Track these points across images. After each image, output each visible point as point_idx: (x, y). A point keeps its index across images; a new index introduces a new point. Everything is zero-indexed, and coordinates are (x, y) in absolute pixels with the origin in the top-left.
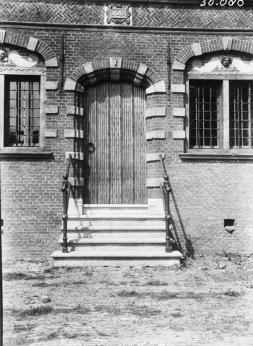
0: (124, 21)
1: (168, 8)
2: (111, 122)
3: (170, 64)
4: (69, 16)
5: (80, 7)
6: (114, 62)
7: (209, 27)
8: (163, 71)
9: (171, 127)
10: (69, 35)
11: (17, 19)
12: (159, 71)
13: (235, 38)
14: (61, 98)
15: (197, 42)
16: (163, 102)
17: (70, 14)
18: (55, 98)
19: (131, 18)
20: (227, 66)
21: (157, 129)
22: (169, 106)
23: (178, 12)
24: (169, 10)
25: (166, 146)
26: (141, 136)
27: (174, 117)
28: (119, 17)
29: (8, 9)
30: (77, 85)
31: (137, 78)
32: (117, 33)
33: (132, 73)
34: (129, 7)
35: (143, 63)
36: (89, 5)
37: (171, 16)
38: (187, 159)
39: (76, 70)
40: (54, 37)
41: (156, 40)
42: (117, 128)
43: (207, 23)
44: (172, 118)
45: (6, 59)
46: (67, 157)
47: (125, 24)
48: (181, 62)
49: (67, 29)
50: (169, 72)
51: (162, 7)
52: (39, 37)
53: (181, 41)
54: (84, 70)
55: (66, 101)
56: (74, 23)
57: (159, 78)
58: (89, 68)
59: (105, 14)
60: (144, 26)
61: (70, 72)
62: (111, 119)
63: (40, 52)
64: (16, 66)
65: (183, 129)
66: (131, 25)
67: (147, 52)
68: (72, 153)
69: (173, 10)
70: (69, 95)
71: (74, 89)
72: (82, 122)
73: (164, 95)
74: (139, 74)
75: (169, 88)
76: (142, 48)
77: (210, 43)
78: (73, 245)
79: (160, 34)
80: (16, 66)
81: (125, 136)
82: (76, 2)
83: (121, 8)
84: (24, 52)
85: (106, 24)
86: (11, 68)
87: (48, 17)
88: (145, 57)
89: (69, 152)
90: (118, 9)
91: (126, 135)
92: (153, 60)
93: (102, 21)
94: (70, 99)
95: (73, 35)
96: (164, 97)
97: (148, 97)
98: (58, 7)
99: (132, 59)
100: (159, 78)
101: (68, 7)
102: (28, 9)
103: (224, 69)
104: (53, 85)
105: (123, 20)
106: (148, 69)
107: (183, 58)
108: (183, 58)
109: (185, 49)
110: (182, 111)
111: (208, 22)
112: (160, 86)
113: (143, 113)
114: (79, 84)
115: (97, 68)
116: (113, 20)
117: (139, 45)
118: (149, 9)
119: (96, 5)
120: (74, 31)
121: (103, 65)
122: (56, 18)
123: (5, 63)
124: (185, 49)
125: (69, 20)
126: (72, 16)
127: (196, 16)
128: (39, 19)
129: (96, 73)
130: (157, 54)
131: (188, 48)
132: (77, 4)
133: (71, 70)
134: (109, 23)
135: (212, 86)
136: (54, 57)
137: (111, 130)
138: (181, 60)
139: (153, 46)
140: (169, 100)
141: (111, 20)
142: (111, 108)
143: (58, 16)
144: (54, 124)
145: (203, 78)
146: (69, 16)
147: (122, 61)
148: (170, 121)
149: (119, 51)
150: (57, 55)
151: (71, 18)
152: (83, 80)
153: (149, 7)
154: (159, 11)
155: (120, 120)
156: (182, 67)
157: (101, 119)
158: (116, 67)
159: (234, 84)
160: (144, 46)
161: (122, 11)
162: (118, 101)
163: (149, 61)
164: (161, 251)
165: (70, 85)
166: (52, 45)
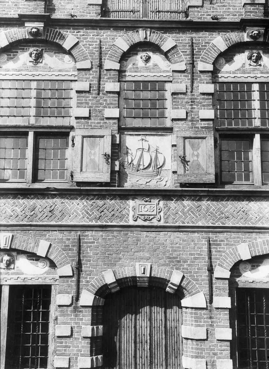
0: (154, 218)
1: (207, 200)
2: (138, 340)
3: (211, 270)
4: (88, 213)
5: (100, 202)
7: (259, 223)
8: (203, 280)
9: (214, 354)
10: (87, 236)
11: (26, 219)
12: (197, 280)
14: (76, 316)
15: (245, 242)
16: (202, 320)
17: (88, 211)
18: (68, 315)
19: (162, 214)
21: (197, 357)
22: (211, 326)
23: (220, 205)
24: (209, 202)
26: (176, 359)
27: (218, 340)
28: (148, 213)
29: (17, 208)
30: (95, 297)
31: (170, 287)
32: (145, 233)
33: (164, 282)
34: (159, 201)
35: (177, 269)
36: (111, 200)
37: (211, 210)
39: (94, 279)
40: (69, 239)
41: (193, 241)
42: (146, 349)
43: (257, 218)
44: (215, 342)
45: (12, 266)
47: (155, 223)
48: (225, 268)
49: (84, 229)
51: (200, 200)
52: (52, 240)
53: (224, 241)
54: (104, 279)
55: (82, 319)
56: (93, 221)
57: (197, 288)
58: (110, 279)
59: (131, 209)
60: (177, 224)
61: (88, 282)
62: (138, 336)
63: (52, 257)
64: (23, 274)
65: (229, 357)
66: (162, 223)
67: (182, 255)
69: (214, 202)
70: (86, 312)
71: (91, 304)
73: (204, 311)
74: (172, 284)
75: (211, 301)
76: (175, 251)
79: (198, 232)
80: (23, 274)
81: (156, 360)
82: (96, 197)
83: (150, 202)
84: (33, 256)
85: (131, 223)
86: (17, 276)
88: (179, 262)
90: (146, 203)
91: (156, 357)
92: (189, 265)
93: (127, 218)
94: (87, 316)
95: (92, 236)
96: (204, 314)
97: (184, 310)
98: (74, 203)
99: (163, 265)
100: (197, 288)
101: (87, 203)
102: (40, 207)
105: (153, 217)
106: (184, 277)
107: (227, 263)
108: (227, 263)
109: (230, 251)
110: (227, 334)
111: (258, 217)
113: (178, 329)
114: (97, 297)
116: (140, 216)
117: (172, 247)
118: (184, 202)
119: (120, 200)
120: (92, 231)
121: (127, 272)
122: (72, 216)
123: (12, 271)
124: (230, 251)
125: (88, 218)
126: (90, 213)
127: (242, 210)
128: (53, 217)
129: (119, 282)
130: (195, 258)
131: (233, 249)
132: (98, 199)
133: (88, 279)
134: (136, 221)
136: (68, 263)
137: (138, 351)
138: (225, 266)
139: (190, 248)
140: (211, 318)
141: (138, 217)
142: (138, 321)
143: (75, 213)
144: (65, 350)
145: (253, 286)
146: (88, 213)
147: (151, 268)
148: (213, 346)
149: (147, 255)
150: (73, 260)
151: (90, 215)
152: (103, 292)
153: (183, 200)
154: (196, 204)
155: (148, 337)
156: (227, 274)
157: (125, 335)
158: (143, 275)
160: (179, 247)
161: (151, 206)
162: (146, 313)
163: (185, 267)
165: (87, 298)
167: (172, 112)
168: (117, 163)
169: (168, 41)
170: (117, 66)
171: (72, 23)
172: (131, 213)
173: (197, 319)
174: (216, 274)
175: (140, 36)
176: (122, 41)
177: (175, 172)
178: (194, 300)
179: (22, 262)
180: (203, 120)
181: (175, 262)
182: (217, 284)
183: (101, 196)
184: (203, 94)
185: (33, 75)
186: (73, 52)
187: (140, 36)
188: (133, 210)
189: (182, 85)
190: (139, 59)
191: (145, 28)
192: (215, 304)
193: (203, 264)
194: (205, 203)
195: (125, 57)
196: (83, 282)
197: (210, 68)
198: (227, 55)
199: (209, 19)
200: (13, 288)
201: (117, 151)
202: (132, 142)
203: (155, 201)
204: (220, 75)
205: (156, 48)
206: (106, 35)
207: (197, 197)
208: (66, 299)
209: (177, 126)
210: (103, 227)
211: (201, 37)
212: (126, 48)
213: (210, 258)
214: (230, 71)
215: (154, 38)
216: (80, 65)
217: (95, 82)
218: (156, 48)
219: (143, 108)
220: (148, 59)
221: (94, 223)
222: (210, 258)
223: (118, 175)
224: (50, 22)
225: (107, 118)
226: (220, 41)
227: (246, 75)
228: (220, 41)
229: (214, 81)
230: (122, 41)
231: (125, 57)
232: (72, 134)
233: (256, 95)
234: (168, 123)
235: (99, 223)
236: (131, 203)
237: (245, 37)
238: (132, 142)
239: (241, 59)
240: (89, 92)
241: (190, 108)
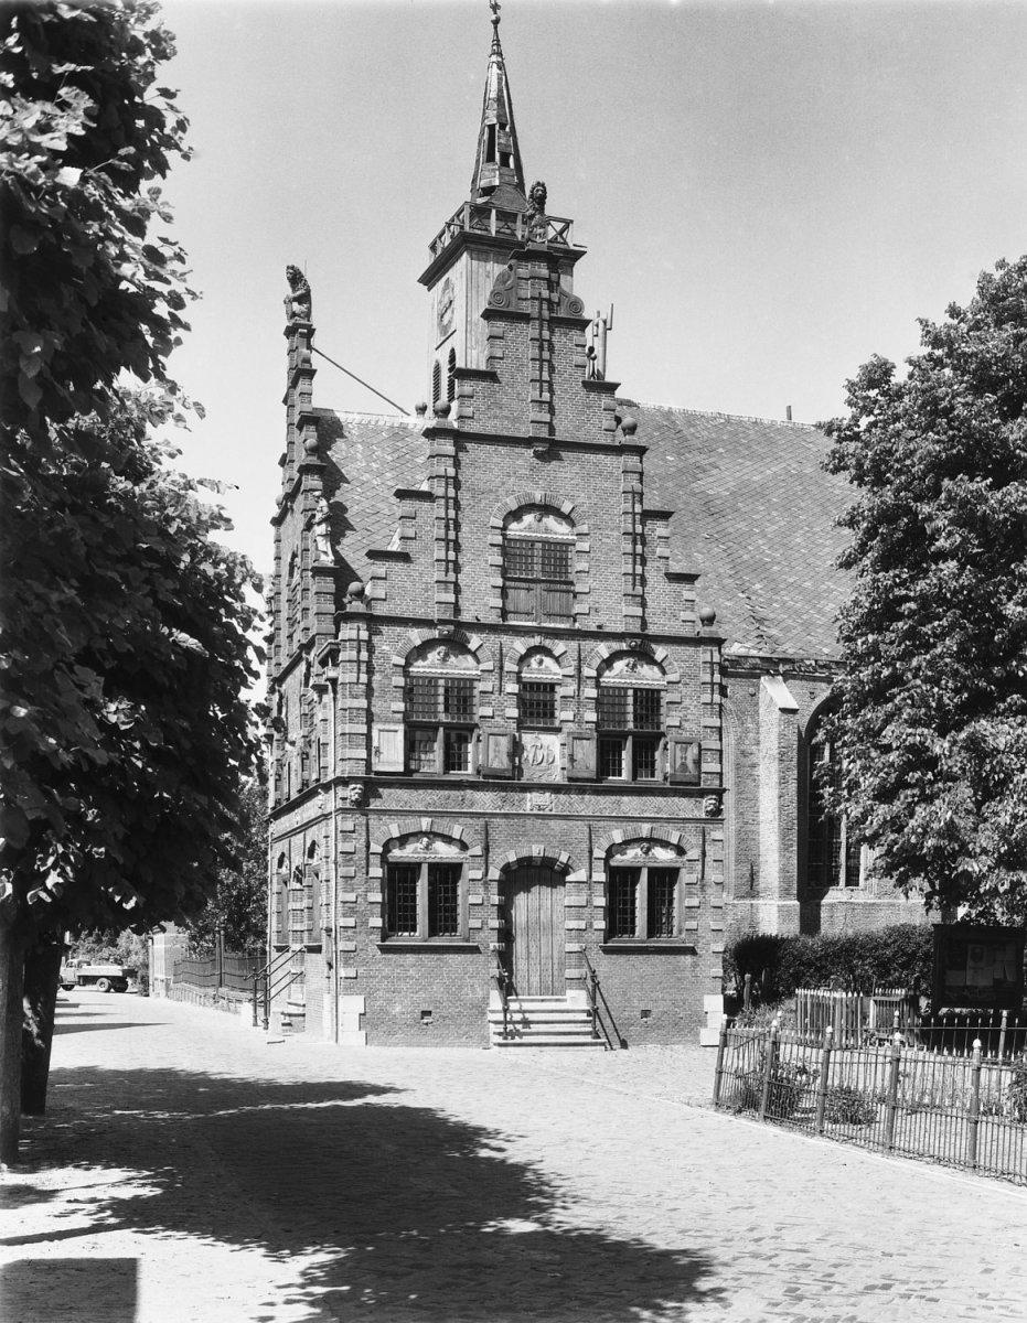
3: (591, 852)
5: (504, 794)
6: (536, 850)
13: (654, 825)
20: (646, 853)
25: (586, 935)
38: (607, 951)
46: (492, 948)
47: (547, 812)
50: (591, 859)
58: (512, 858)
68: (497, 944)
72: (504, 911)
75: (591, 877)
77: (631, 830)
78: (512, 1034)
84: (448, 840)
87: (472, 805)
89: (494, 945)
94: (494, 888)
103: (644, 855)
104: (478, 874)
110: (601, 901)
115: (520, 856)
121: (524, 853)
129: (520, 861)
159: (653, 872)
164: (589, 1039)
165: (495, 874)
167: (563, 714)
168: (517, 759)
169: (559, 647)
170: (516, 669)
171: (479, 627)
172: (529, 804)
173: (579, 891)
174: (595, 855)
175: (536, 641)
176: (520, 645)
177: (563, 769)
178: (580, 875)
179: (439, 846)
180: (587, 722)
181: (564, 844)
182: (595, 863)
183: (503, 788)
184: (587, 698)
185: (442, 673)
186: (478, 653)
187: (536, 641)
188: (532, 801)
189: (569, 689)
190: (534, 661)
191: (540, 633)
192: (594, 879)
193: (585, 846)
194: (587, 797)
195: (523, 659)
196: (490, 860)
197: (594, 674)
198: (607, 664)
200: (430, 865)
201: (517, 748)
202: (528, 739)
203: (548, 794)
204: (601, 680)
205: (548, 652)
206: (505, 638)
207: (582, 791)
208: (478, 874)
209: (568, 727)
210: (506, 816)
211: (588, 645)
212: (523, 651)
213: (591, 842)
214: (610, 678)
215: (548, 643)
216: (482, 667)
217: (497, 683)
218: (548, 652)
219: (537, 705)
220: (541, 662)
221: (498, 811)
222: (591, 842)
223: (517, 770)
224: (460, 625)
225: (508, 718)
226: (604, 649)
227: (623, 681)
228: (604, 649)
229: (598, 686)
230: (520, 645)
231: (523, 659)
232: (476, 732)
233: (630, 700)
234: (557, 724)
235: (503, 811)
236: (528, 795)
237: (624, 646)
238: (528, 739)
239: (620, 665)
240: (492, 693)
241: (576, 713)
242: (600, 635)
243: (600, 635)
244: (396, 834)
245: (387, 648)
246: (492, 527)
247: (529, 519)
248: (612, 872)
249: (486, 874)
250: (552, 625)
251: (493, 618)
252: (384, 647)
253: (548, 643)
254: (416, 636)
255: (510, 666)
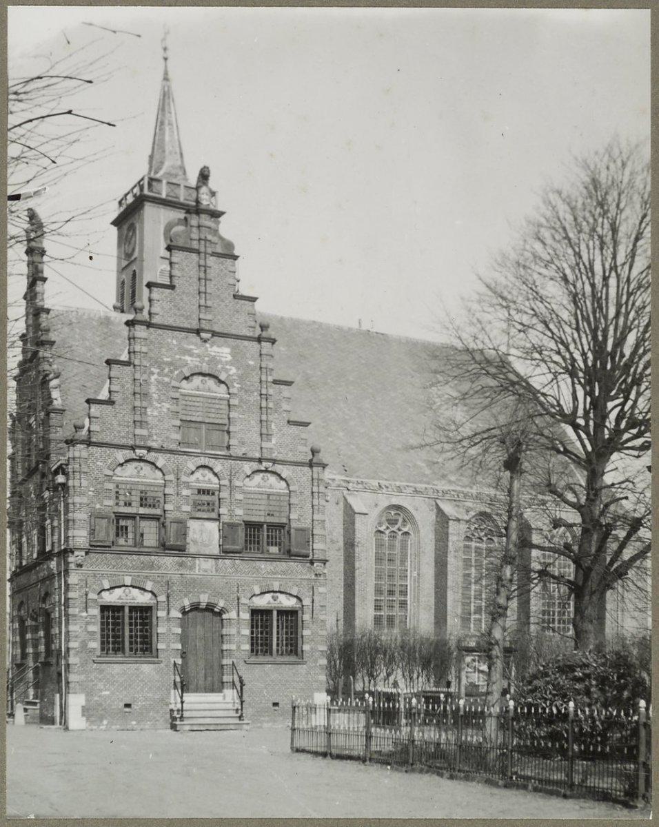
66: (214, 573)
75: (238, 615)
87: (159, 568)
110: (247, 632)
112: (233, 615)
115: (191, 602)
121: (195, 600)
135: (266, 613)
166: (162, 586)
176: (191, 464)
187: (204, 461)
190: (198, 475)
199: (240, 455)
206: (182, 458)
215: (211, 462)
242: (244, 458)
243: (244, 458)
244: (107, 587)
245: (101, 464)
246: (173, 387)
247: (197, 380)
248: (255, 612)
249: (168, 614)
250: (213, 452)
251: (173, 447)
252: (99, 463)
253: (211, 462)
254: (121, 456)
255: (184, 478)
